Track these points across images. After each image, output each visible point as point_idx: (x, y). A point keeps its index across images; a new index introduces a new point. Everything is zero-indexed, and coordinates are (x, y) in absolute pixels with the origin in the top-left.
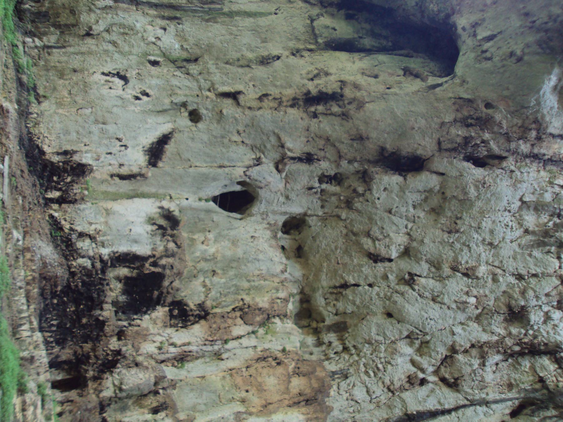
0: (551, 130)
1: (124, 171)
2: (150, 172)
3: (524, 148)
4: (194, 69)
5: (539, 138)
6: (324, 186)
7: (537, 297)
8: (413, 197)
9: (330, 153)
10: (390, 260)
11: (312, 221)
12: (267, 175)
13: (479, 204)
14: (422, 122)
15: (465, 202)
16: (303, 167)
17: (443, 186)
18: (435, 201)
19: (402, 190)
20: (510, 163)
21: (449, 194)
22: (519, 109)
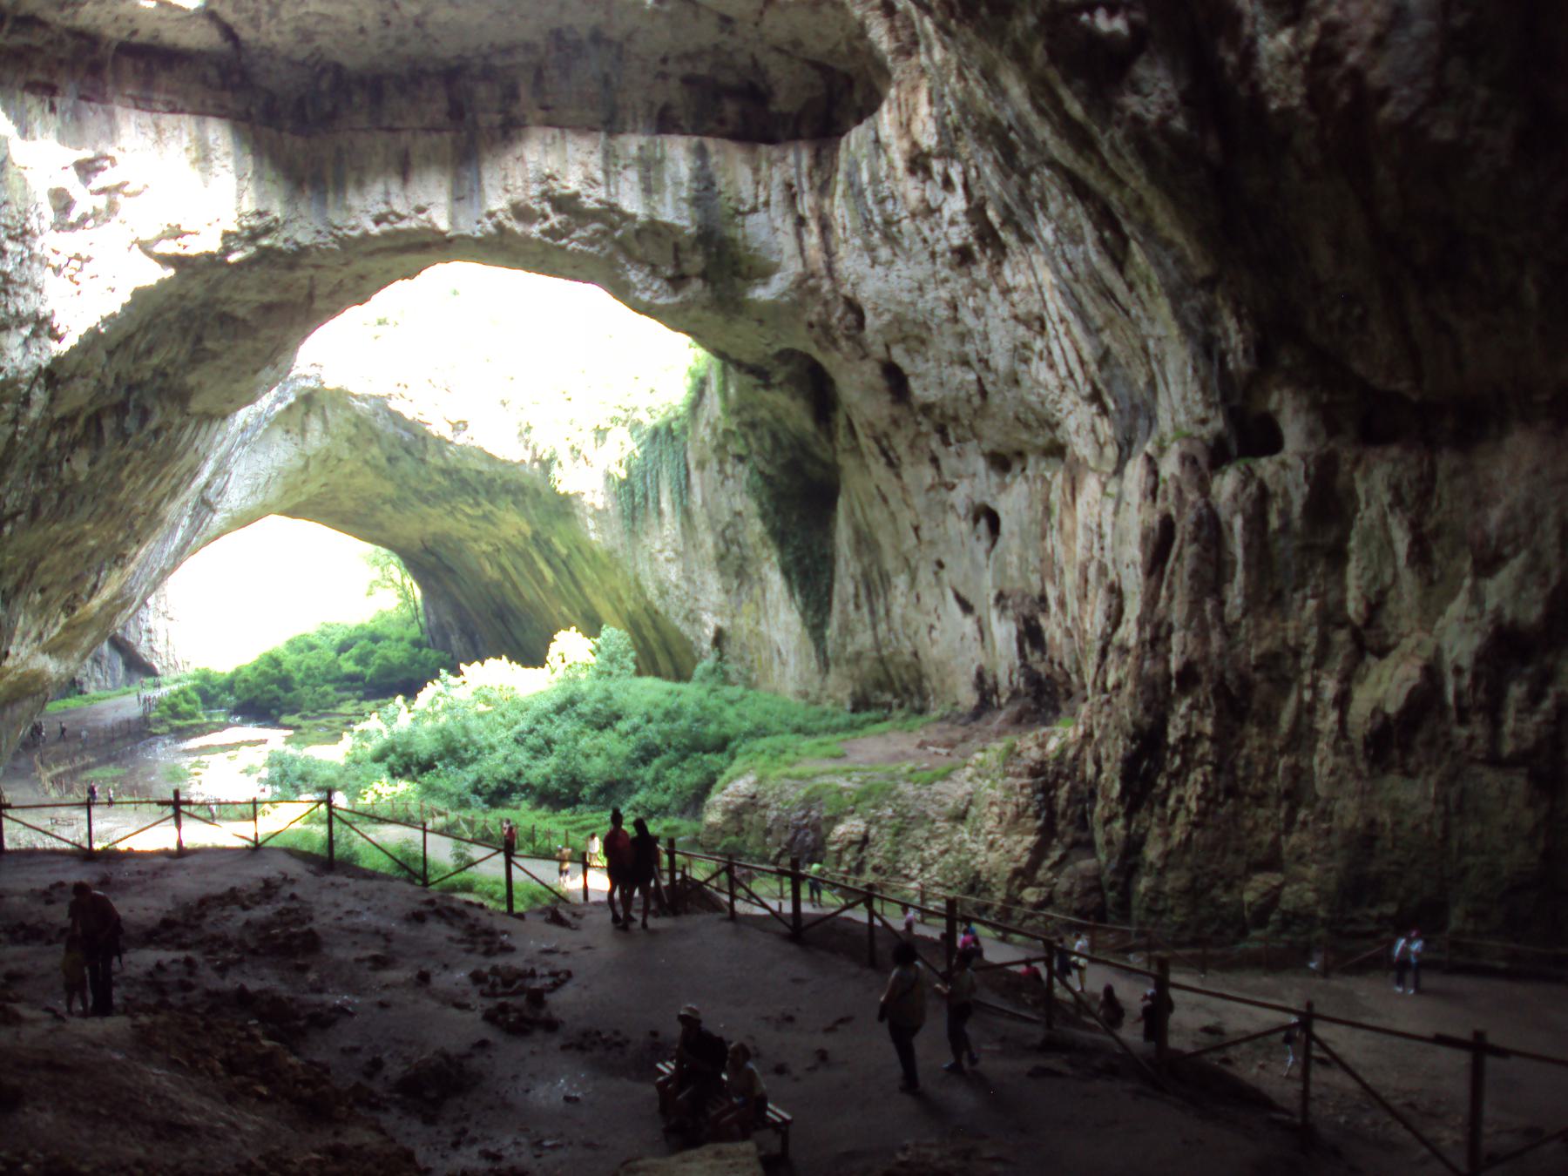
0: (800, 269)
1: (978, 637)
2: (978, 612)
3: (826, 285)
4: (913, 563)
5: (812, 275)
6: (952, 440)
7: (938, 240)
8: (921, 366)
9: (921, 442)
10: (979, 380)
11: (987, 447)
12: (960, 496)
13: (893, 307)
14: (854, 376)
15: (898, 320)
16: (944, 463)
17: (897, 342)
18: (914, 344)
19: (918, 376)
20: (846, 290)
21: (899, 336)
22: (797, 306)
